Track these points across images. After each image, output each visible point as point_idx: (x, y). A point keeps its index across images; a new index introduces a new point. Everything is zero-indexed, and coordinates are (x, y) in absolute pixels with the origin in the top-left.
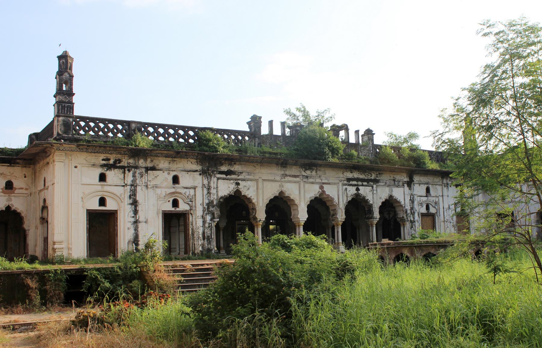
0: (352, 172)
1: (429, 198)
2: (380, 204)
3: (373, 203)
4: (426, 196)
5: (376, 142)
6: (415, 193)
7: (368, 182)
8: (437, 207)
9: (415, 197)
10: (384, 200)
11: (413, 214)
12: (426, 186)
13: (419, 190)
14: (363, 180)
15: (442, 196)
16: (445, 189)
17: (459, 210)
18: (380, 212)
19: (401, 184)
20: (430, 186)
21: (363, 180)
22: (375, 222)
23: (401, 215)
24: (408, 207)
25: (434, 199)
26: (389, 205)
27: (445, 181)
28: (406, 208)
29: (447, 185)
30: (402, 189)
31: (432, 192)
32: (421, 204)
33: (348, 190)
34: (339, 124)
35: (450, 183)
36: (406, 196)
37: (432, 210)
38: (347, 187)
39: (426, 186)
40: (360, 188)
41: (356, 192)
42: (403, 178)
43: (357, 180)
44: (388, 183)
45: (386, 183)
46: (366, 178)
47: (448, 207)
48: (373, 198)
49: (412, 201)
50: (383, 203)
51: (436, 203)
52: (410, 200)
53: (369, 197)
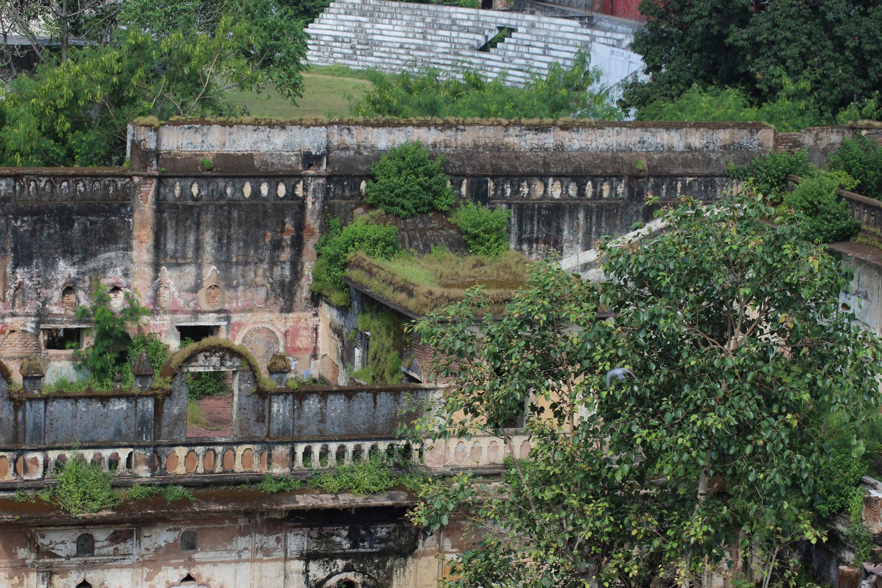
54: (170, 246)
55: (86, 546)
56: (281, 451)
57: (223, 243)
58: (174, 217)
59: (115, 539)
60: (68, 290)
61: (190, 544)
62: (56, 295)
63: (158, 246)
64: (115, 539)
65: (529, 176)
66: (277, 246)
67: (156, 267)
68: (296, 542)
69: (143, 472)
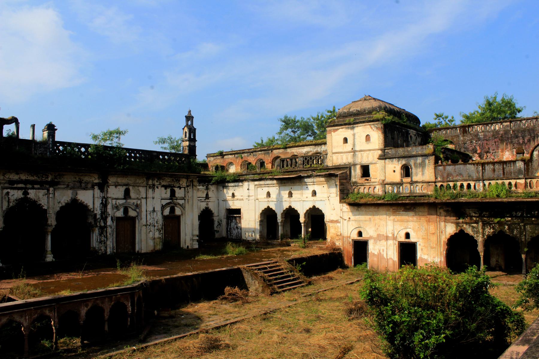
0: (17, 174)
1: (129, 201)
2: (58, 209)
3: (48, 208)
4: (125, 198)
5: (57, 139)
6: (109, 195)
7: (42, 185)
8: (138, 210)
9: (110, 200)
10: (64, 204)
11: (105, 219)
12: (125, 187)
13: (115, 193)
14: (33, 183)
15: (146, 198)
16: (150, 191)
17: (167, 212)
18: (57, 219)
19: (90, 186)
20: (131, 188)
21: (33, 183)
22: (50, 229)
23: (91, 220)
24: (98, 212)
25: (135, 201)
26: (75, 211)
27: (150, 182)
28: (96, 212)
29: (153, 187)
30: (90, 192)
31: (133, 194)
32: (117, 208)
33: (10, 194)
34: (7, 116)
35: (156, 184)
36: (96, 200)
37: (132, 213)
38: (9, 190)
39: (125, 187)
40: (30, 191)
41: (23, 196)
42: (94, 179)
43: (26, 182)
44: (71, 185)
45: (68, 186)
46: (39, 180)
47: (152, 209)
48: (48, 202)
49: (104, 205)
50: (62, 208)
51: (137, 206)
52: (102, 203)
53: (43, 202)
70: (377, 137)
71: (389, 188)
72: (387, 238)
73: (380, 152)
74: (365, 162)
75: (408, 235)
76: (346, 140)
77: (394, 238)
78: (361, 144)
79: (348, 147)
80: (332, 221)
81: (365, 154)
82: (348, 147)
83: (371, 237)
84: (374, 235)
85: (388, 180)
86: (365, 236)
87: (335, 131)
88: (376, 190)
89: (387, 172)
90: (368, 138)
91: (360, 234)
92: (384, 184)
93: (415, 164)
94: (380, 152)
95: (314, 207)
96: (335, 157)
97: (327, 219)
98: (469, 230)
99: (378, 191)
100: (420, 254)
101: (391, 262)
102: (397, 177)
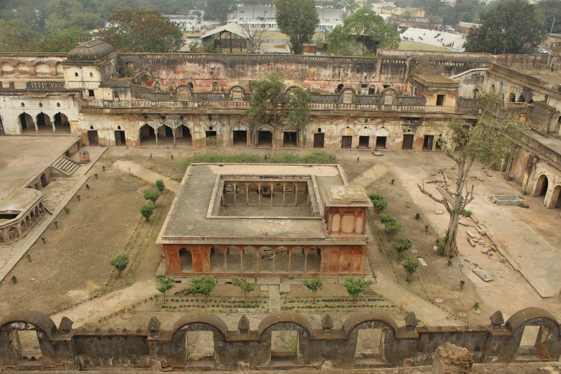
54: (383, 71)
55: (366, 121)
56: (400, 107)
57: (392, 71)
58: (384, 66)
59: (371, 120)
60: (365, 78)
61: (384, 122)
62: (363, 78)
63: (381, 71)
64: (371, 120)
65: (446, 61)
66: (401, 72)
67: (380, 74)
68: (402, 122)
69: (377, 109)
70: (97, 76)
71: (106, 103)
72: (108, 129)
73: (99, 83)
74: (91, 88)
75: (119, 127)
76: (77, 75)
77: (112, 129)
78: (87, 77)
79: (79, 79)
80: (73, 121)
81: (90, 83)
82: (79, 79)
83: (99, 129)
84: (101, 128)
85: (105, 99)
86: (95, 128)
87: (69, 68)
88: (99, 104)
89: (104, 95)
90: (91, 74)
91: (92, 127)
92: (104, 101)
93: (120, 91)
94: (99, 83)
95: (59, 113)
96: (70, 84)
97: (70, 119)
98: (150, 123)
99: (101, 104)
100: (127, 136)
101: (111, 142)
102: (110, 97)
